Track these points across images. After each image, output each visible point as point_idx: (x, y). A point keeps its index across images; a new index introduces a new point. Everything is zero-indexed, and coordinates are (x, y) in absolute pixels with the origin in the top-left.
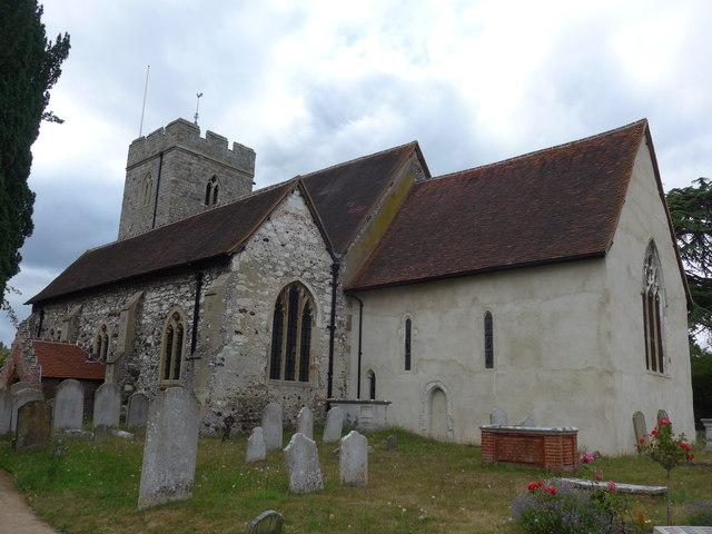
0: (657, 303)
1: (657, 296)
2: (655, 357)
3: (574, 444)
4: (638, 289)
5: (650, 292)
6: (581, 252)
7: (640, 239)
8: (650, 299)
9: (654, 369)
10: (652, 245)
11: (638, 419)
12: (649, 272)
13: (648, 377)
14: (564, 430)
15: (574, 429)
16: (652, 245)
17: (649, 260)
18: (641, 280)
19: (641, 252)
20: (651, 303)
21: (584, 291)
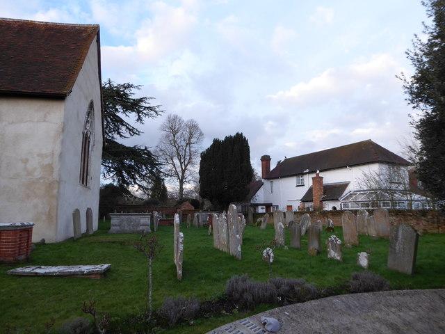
0: (89, 142)
1: (89, 138)
2: (84, 177)
3: (29, 237)
4: (82, 129)
5: (87, 134)
6: (48, 91)
7: (86, 98)
8: (86, 138)
9: (83, 183)
10: (91, 105)
11: (76, 214)
12: (88, 121)
13: (80, 188)
14: (23, 225)
15: (31, 223)
16: (91, 105)
17: (89, 114)
18: (83, 124)
19: (85, 108)
20: (86, 140)
21: (45, 121)
